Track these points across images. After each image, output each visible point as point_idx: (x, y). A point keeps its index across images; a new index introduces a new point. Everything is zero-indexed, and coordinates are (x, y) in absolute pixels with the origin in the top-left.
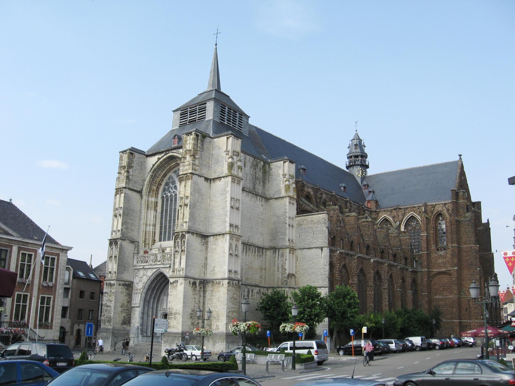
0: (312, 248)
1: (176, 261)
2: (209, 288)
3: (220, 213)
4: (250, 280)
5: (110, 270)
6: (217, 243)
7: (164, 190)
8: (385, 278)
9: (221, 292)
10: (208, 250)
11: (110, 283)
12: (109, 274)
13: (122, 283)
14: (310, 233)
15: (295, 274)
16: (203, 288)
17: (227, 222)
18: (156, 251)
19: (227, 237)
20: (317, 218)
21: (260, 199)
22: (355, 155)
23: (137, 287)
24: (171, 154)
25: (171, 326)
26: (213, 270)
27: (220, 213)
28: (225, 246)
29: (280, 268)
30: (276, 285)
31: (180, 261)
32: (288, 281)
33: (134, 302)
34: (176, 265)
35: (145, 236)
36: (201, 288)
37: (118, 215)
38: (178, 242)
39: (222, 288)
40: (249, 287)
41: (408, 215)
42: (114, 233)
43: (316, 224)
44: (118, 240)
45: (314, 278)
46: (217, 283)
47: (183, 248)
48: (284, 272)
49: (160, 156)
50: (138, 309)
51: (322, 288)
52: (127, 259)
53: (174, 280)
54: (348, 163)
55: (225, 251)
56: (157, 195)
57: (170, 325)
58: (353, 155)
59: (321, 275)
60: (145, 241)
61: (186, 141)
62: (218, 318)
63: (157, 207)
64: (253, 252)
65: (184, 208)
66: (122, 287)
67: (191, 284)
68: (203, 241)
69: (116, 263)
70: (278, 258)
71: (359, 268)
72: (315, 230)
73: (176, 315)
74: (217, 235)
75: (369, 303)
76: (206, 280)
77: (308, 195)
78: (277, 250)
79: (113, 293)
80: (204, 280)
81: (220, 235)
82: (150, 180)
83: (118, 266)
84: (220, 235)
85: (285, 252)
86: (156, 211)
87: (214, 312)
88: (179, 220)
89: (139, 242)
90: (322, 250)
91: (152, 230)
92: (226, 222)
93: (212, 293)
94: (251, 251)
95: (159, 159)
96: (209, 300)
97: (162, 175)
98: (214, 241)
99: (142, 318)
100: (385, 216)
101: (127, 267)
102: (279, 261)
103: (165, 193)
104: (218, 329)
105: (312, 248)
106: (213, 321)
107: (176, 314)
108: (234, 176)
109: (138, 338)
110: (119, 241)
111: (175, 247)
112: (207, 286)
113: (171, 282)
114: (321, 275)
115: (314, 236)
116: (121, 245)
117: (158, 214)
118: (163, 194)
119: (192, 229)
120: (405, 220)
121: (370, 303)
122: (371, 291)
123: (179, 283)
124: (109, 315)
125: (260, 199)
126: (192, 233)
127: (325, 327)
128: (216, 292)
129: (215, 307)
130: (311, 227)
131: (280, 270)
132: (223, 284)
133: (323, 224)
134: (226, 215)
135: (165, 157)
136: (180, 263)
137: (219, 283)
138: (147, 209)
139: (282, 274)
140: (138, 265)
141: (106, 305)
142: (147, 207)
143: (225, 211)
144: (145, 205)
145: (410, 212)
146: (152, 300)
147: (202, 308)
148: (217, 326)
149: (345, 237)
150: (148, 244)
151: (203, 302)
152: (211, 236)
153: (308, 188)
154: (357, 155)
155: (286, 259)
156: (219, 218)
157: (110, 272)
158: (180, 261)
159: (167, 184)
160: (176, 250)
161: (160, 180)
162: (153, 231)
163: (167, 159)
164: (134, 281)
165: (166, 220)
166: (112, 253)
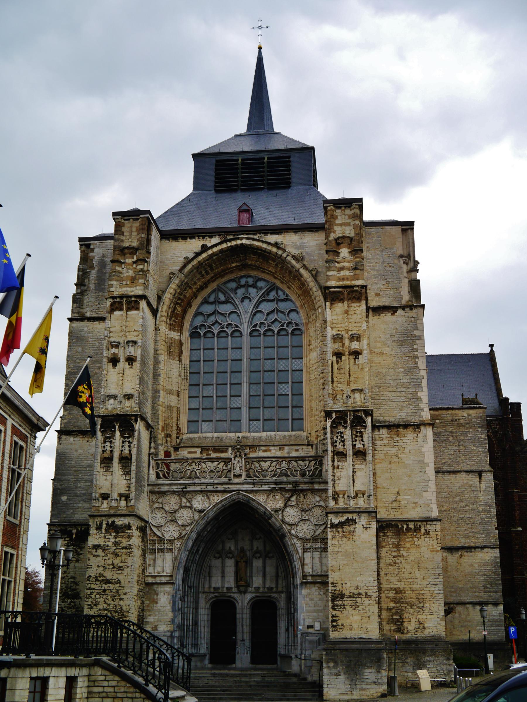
1: (337, 474)
3: (402, 381)
5: (104, 491)
6: (401, 443)
9: (423, 549)
11: (113, 522)
12: (105, 502)
14: (450, 442)
17: (423, 402)
18: (195, 452)
19: (429, 432)
24: (244, 241)
25: (342, 625)
26: (396, 501)
27: (402, 381)
28: (423, 450)
34: (339, 484)
38: (341, 433)
39: (427, 539)
43: (463, 426)
44: (133, 418)
45: (465, 530)
46: (408, 529)
47: (339, 446)
49: (210, 242)
50: (168, 588)
51: (486, 550)
53: (343, 519)
55: (426, 461)
57: (340, 623)
59: (481, 523)
62: (421, 605)
72: (463, 438)
73: (359, 600)
74: (397, 426)
79: (126, 548)
81: (406, 426)
84: (406, 426)
87: (409, 593)
90: (480, 478)
92: (419, 400)
93: (399, 551)
95: (205, 248)
96: (390, 565)
97: (200, 283)
98: (391, 437)
104: (424, 628)
106: (408, 613)
110: (136, 421)
111: (334, 444)
112: (381, 534)
114: (481, 523)
115: (461, 448)
123: (359, 526)
124: (116, 602)
127: (498, 626)
128: (409, 549)
129: (411, 580)
130: (451, 432)
132: (427, 533)
133: (479, 427)
134: (419, 386)
135: (224, 246)
136: (353, 480)
137: (417, 530)
140: (160, 482)
141: (100, 579)
143: (416, 377)
148: (420, 623)
156: (399, 390)
157: (105, 497)
158: (353, 476)
163: (226, 251)
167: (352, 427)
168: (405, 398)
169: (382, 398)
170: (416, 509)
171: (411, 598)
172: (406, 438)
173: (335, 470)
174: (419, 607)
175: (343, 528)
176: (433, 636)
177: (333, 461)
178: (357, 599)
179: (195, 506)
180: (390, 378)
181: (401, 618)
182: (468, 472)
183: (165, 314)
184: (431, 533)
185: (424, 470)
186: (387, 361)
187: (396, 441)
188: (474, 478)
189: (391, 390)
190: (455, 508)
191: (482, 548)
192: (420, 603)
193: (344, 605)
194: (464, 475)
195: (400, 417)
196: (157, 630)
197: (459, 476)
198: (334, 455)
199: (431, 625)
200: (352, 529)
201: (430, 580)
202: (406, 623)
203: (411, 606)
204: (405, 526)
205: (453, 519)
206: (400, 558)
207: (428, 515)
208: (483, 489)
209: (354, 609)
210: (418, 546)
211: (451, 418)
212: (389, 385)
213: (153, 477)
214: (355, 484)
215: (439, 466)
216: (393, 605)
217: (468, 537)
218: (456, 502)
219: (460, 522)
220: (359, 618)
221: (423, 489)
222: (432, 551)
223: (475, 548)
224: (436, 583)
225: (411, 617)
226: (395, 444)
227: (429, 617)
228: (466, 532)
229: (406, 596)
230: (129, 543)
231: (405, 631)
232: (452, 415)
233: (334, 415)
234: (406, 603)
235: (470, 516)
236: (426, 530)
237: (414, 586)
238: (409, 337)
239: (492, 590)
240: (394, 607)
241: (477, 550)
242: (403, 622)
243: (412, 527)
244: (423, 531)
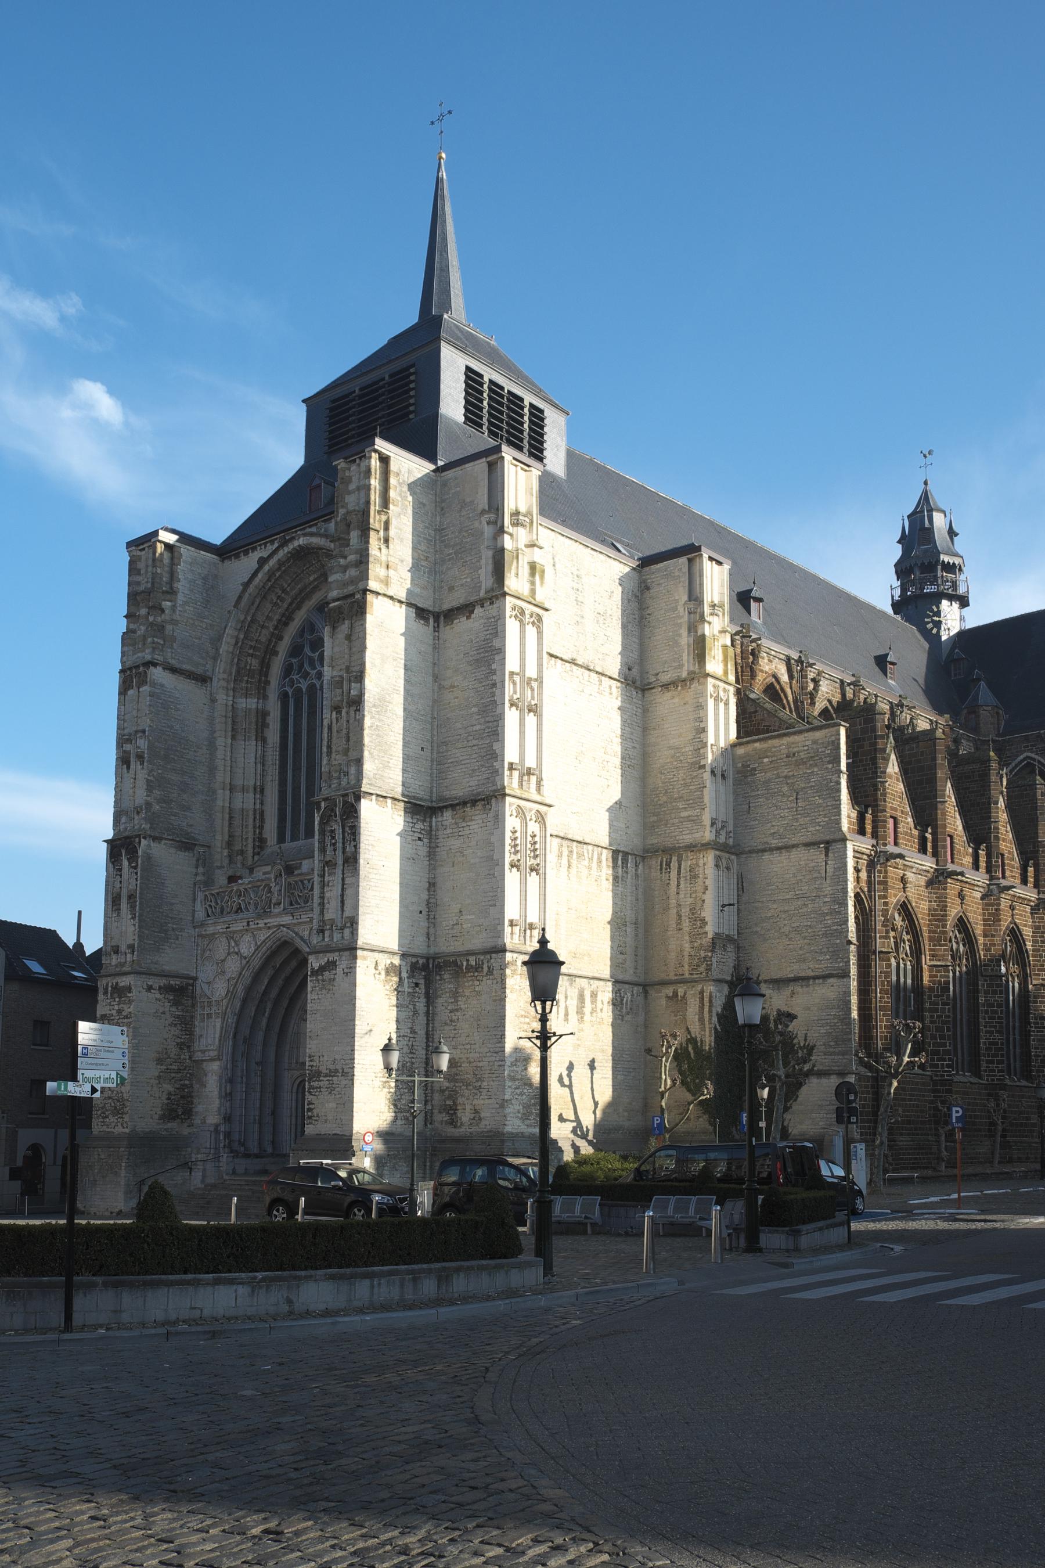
0: (794, 846)
1: (327, 895)
2: (446, 984)
3: (475, 728)
4: (586, 958)
7: (288, 670)
8: (1039, 950)
10: (438, 857)
12: (114, 956)
13: (157, 982)
14: (784, 795)
15: (736, 937)
16: (422, 986)
20: (807, 743)
21: (610, 687)
22: (923, 564)
23: (209, 993)
25: (318, 1116)
27: (475, 728)
29: (683, 918)
30: (672, 974)
31: (342, 896)
32: (714, 960)
33: (199, 1045)
35: (230, 824)
36: (417, 985)
37: (132, 759)
38: (332, 831)
40: (584, 982)
42: (123, 819)
43: (805, 763)
48: (701, 931)
52: (172, 904)
54: (897, 593)
55: (495, 858)
56: (264, 689)
57: (315, 1112)
58: (916, 564)
59: (825, 935)
60: (229, 844)
61: (348, 481)
62: (479, 1084)
63: (266, 730)
64: (594, 865)
65: (348, 713)
66: (158, 996)
67: (383, 973)
68: (419, 826)
69: (133, 918)
70: (678, 886)
71: (953, 914)
72: (803, 785)
75: (986, 1032)
76: (434, 959)
77: (772, 684)
78: (674, 859)
79: (126, 1017)
80: (428, 959)
81: (474, 802)
82: (237, 638)
83: (140, 927)
85: (701, 862)
86: (264, 740)
88: (333, 755)
89: (209, 847)
91: (252, 807)
93: (457, 1001)
94: (586, 863)
96: (446, 1024)
97: (277, 617)
98: (456, 823)
99: (227, 1096)
100: (1027, 757)
101: (173, 929)
102: (682, 896)
103: (292, 681)
104: (480, 1119)
105: (794, 846)
106: (463, 1096)
107: (333, 1073)
108: (518, 598)
109: (219, 1161)
110: (140, 842)
111: (323, 850)
112: (438, 978)
113: (312, 969)
114: (825, 935)
115: (799, 805)
116: (148, 858)
117: (269, 752)
118: (284, 686)
119: (380, 783)
121: (991, 1032)
122: (994, 992)
123: (339, 970)
125: (610, 687)
126: (378, 795)
129: (468, 1047)
130: (786, 777)
131: (686, 925)
133: (829, 762)
136: (342, 902)
137: (478, 968)
138: (233, 738)
139: (694, 936)
142: (233, 729)
144: (226, 723)
146: (260, 1036)
147: (424, 1052)
148: (476, 1112)
149: (902, 812)
150: (242, 852)
151: (427, 1034)
152: (446, 807)
153: (770, 661)
154: (930, 563)
155: (706, 888)
156: (470, 744)
158: (342, 896)
159: (296, 650)
160: (328, 859)
161: (272, 634)
162: (255, 810)
164: (200, 975)
165: (297, 769)
166: (118, 885)
167: (343, 821)
168: (476, 756)
169: (449, 761)
170: (481, 936)
171: (467, 1073)
172: (473, 823)
173: (326, 889)
174: (475, 1088)
175: (323, 975)
176: (490, 1131)
177: (323, 876)
178: (334, 1078)
179: (242, 951)
180: (460, 726)
181: (455, 1104)
182: (808, 845)
183: (225, 676)
184: (495, 972)
185: (492, 872)
186: (457, 698)
187: (461, 829)
188: (817, 856)
189: (460, 746)
190: (785, 912)
191: (825, 977)
192: (477, 1081)
193: (320, 1088)
194: (801, 849)
195: (470, 789)
196: (205, 1122)
197: (795, 854)
198: (324, 867)
199: (488, 1115)
200: (332, 977)
201: (490, 1046)
202: (460, 1111)
203: (467, 1086)
204: (465, 963)
205: (783, 930)
206: (457, 1014)
207: (493, 944)
208: (831, 874)
209: (330, 1093)
210: (479, 993)
211: (786, 751)
212: (459, 737)
213: (200, 914)
214: (345, 908)
215: (765, 840)
216: (447, 1084)
217: (804, 961)
218: (787, 901)
219: (792, 935)
220: (334, 1105)
221: (490, 903)
222: (495, 1001)
223: (815, 978)
224: (497, 1050)
225: (466, 1102)
226: (460, 833)
227: (487, 1101)
228: (801, 952)
229: (461, 1071)
230: (129, 1010)
231: (459, 1124)
232: (788, 746)
233: (323, 805)
234: (462, 1080)
235: (809, 924)
236: (489, 968)
237: (471, 1055)
238: (487, 652)
239: (837, 1050)
240: (447, 1088)
241: (817, 981)
242: (456, 1110)
243: (473, 963)
244: (485, 969)
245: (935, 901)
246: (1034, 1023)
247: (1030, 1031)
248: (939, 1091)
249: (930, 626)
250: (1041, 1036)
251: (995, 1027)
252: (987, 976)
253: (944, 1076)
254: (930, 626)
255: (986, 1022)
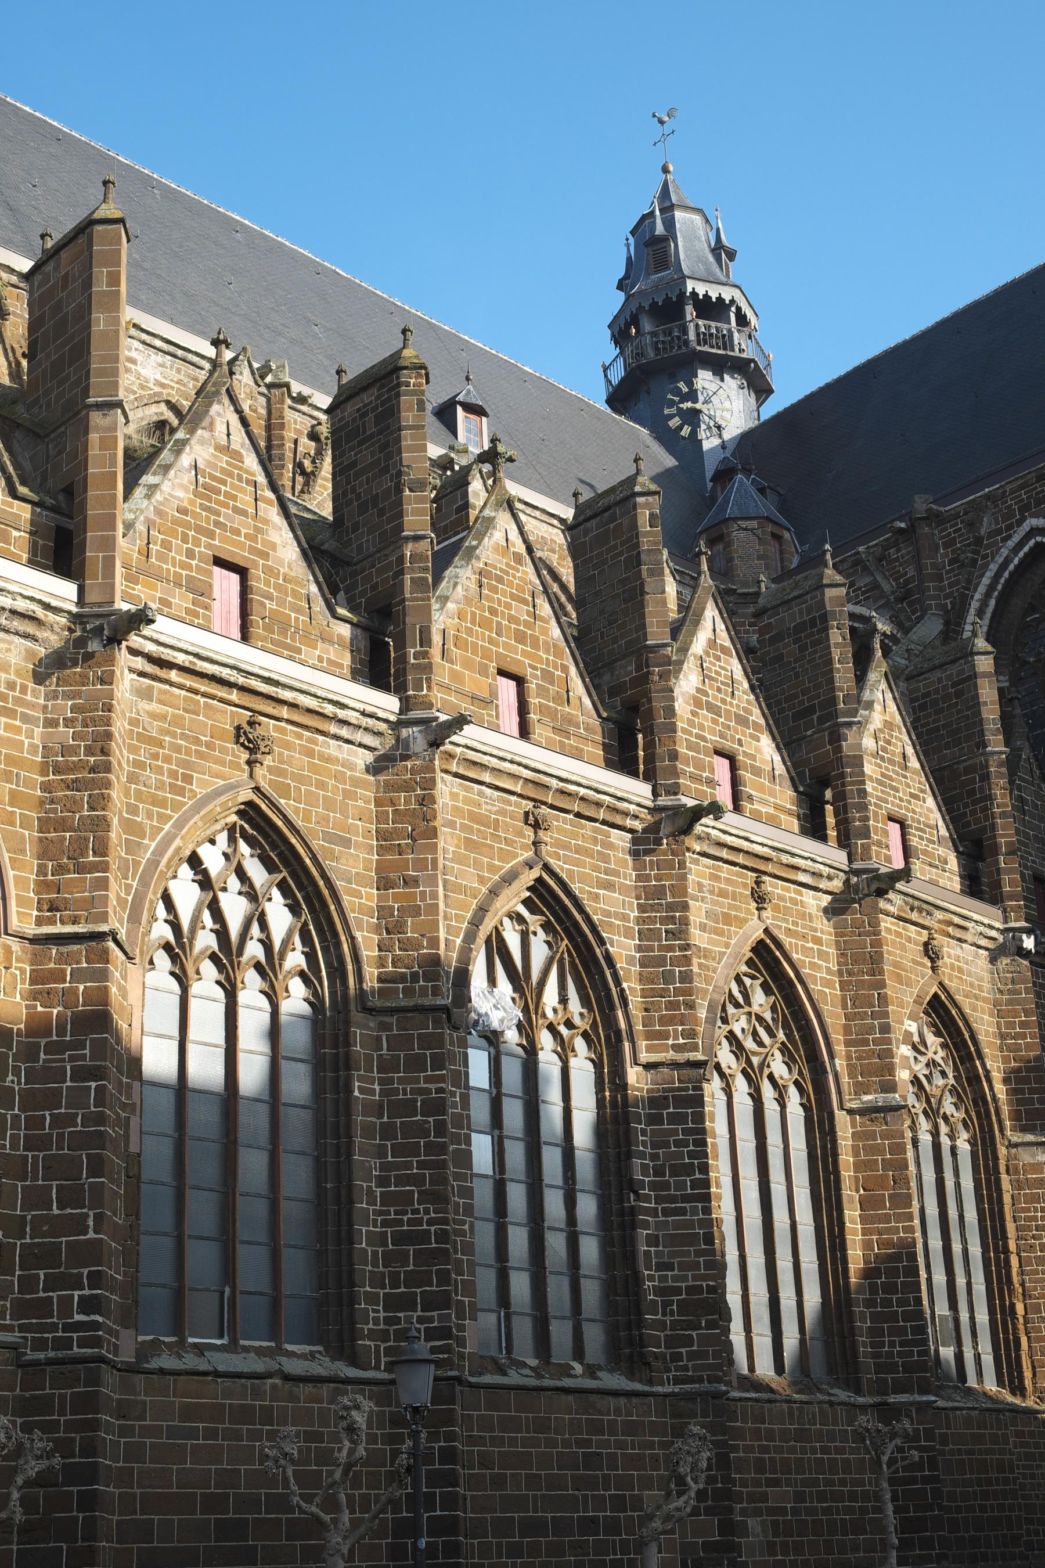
8: (661, 961)
22: (654, 304)
41: (1004, 552)
120: (988, 595)
122: (416, 1064)
145: (1020, 523)
154: (668, 299)
245: (69, 722)
246: (653, 1186)
247: (633, 1211)
248: (44, 1405)
249: (674, 423)
250: (677, 1225)
251: (417, 1180)
252: (391, 1011)
253: (67, 1344)
254: (674, 423)
255: (384, 1167)
